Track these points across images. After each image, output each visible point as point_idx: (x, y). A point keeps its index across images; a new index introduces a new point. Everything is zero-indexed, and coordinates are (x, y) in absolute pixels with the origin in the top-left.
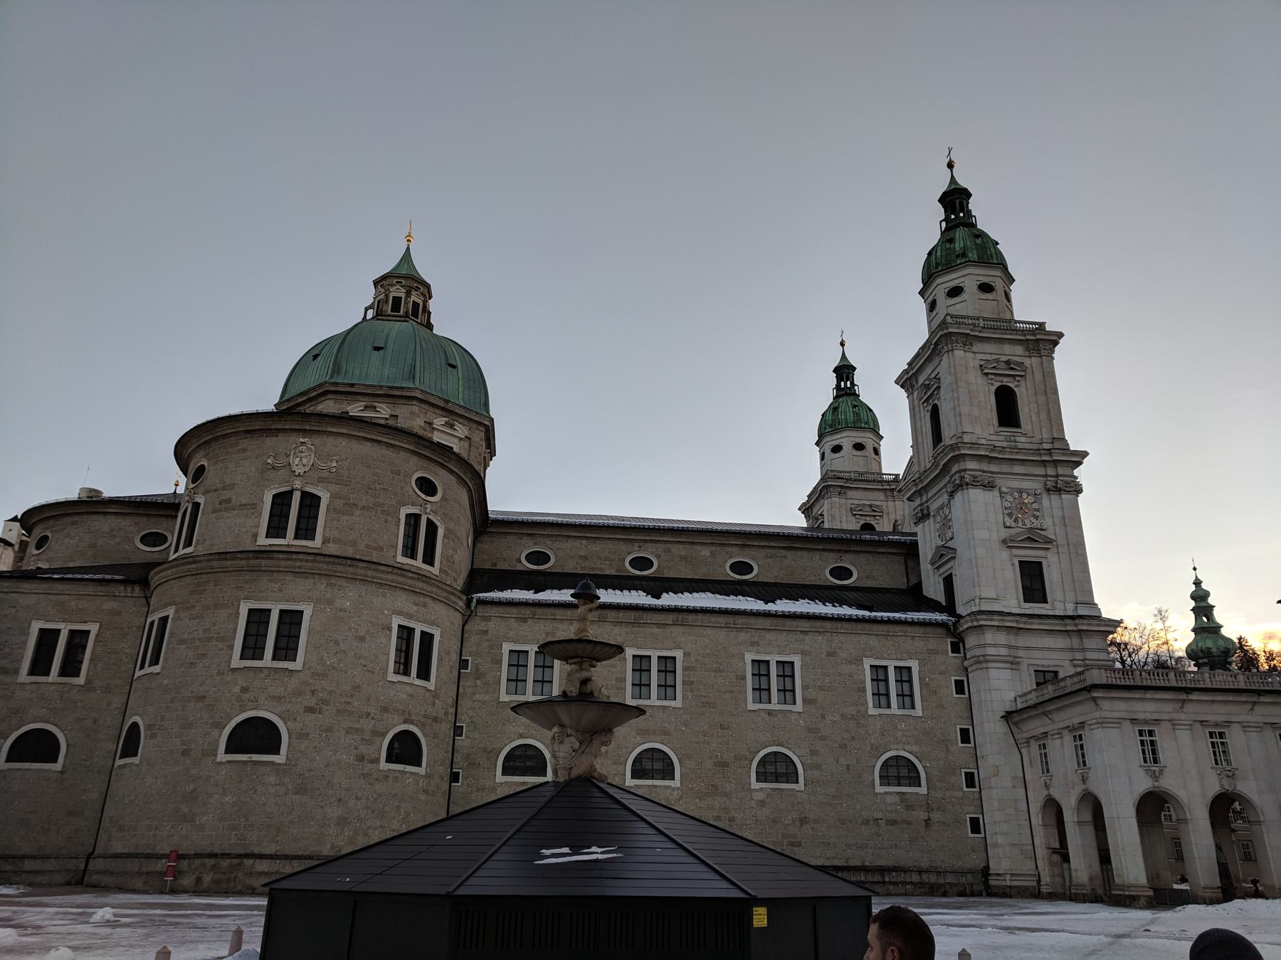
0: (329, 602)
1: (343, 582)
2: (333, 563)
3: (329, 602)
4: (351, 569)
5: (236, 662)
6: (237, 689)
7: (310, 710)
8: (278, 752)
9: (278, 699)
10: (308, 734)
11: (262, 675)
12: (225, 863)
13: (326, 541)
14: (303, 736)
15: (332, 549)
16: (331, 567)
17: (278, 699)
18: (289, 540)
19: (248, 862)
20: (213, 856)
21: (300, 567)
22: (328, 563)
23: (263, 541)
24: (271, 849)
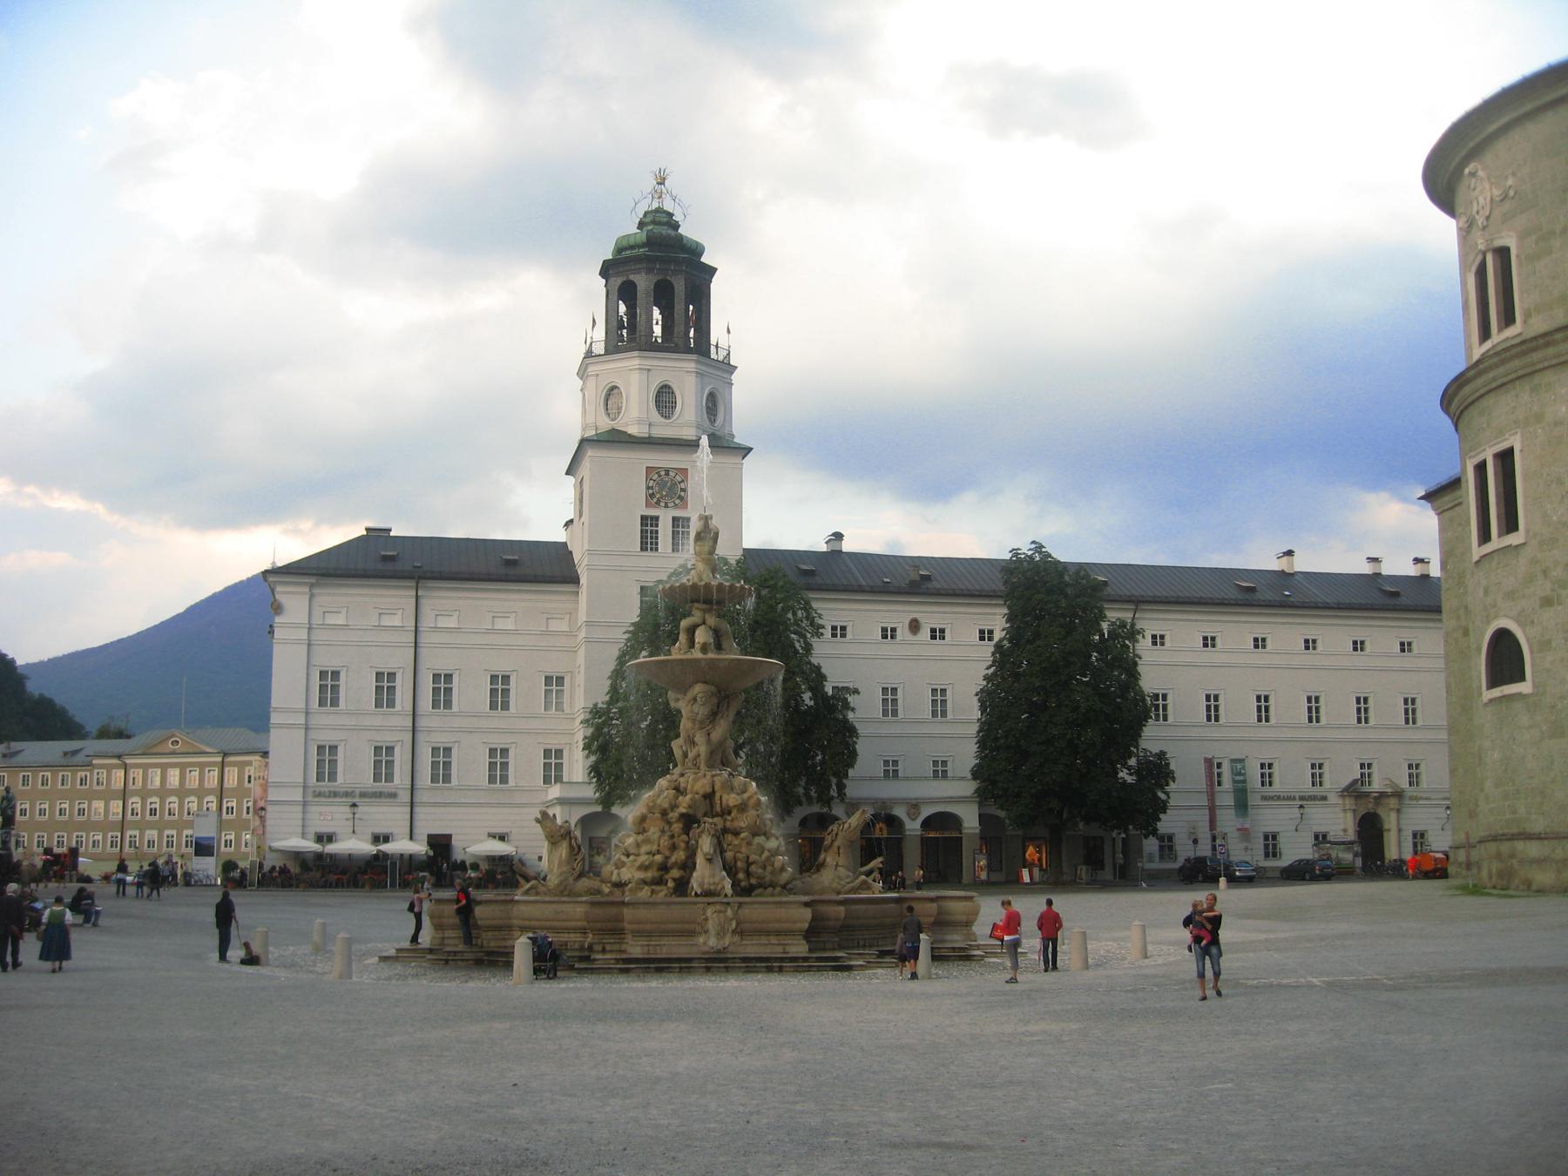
0: (1539, 418)
1: (1549, 376)
2: (1524, 353)
3: (1539, 418)
4: (1551, 351)
5: (1477, 552)
6: (1481, 594)
7: (1547, 602)
8: (1522, 678)
9: (1511, 595)
10: (1549, 641)
11: (1494, 564)
12: (1505, 847)
13: (1527, 316)
14: (1544, 645)
15: (1539, 325)
16: (1528, 359)
17: (1511, 595)
18: (1497, 337)
19: (1520, 845)
20: (1495, 838)
21: (1494, 379)
22: (1517, 356)
23: (1478, 353)
24: (1538, 825)
